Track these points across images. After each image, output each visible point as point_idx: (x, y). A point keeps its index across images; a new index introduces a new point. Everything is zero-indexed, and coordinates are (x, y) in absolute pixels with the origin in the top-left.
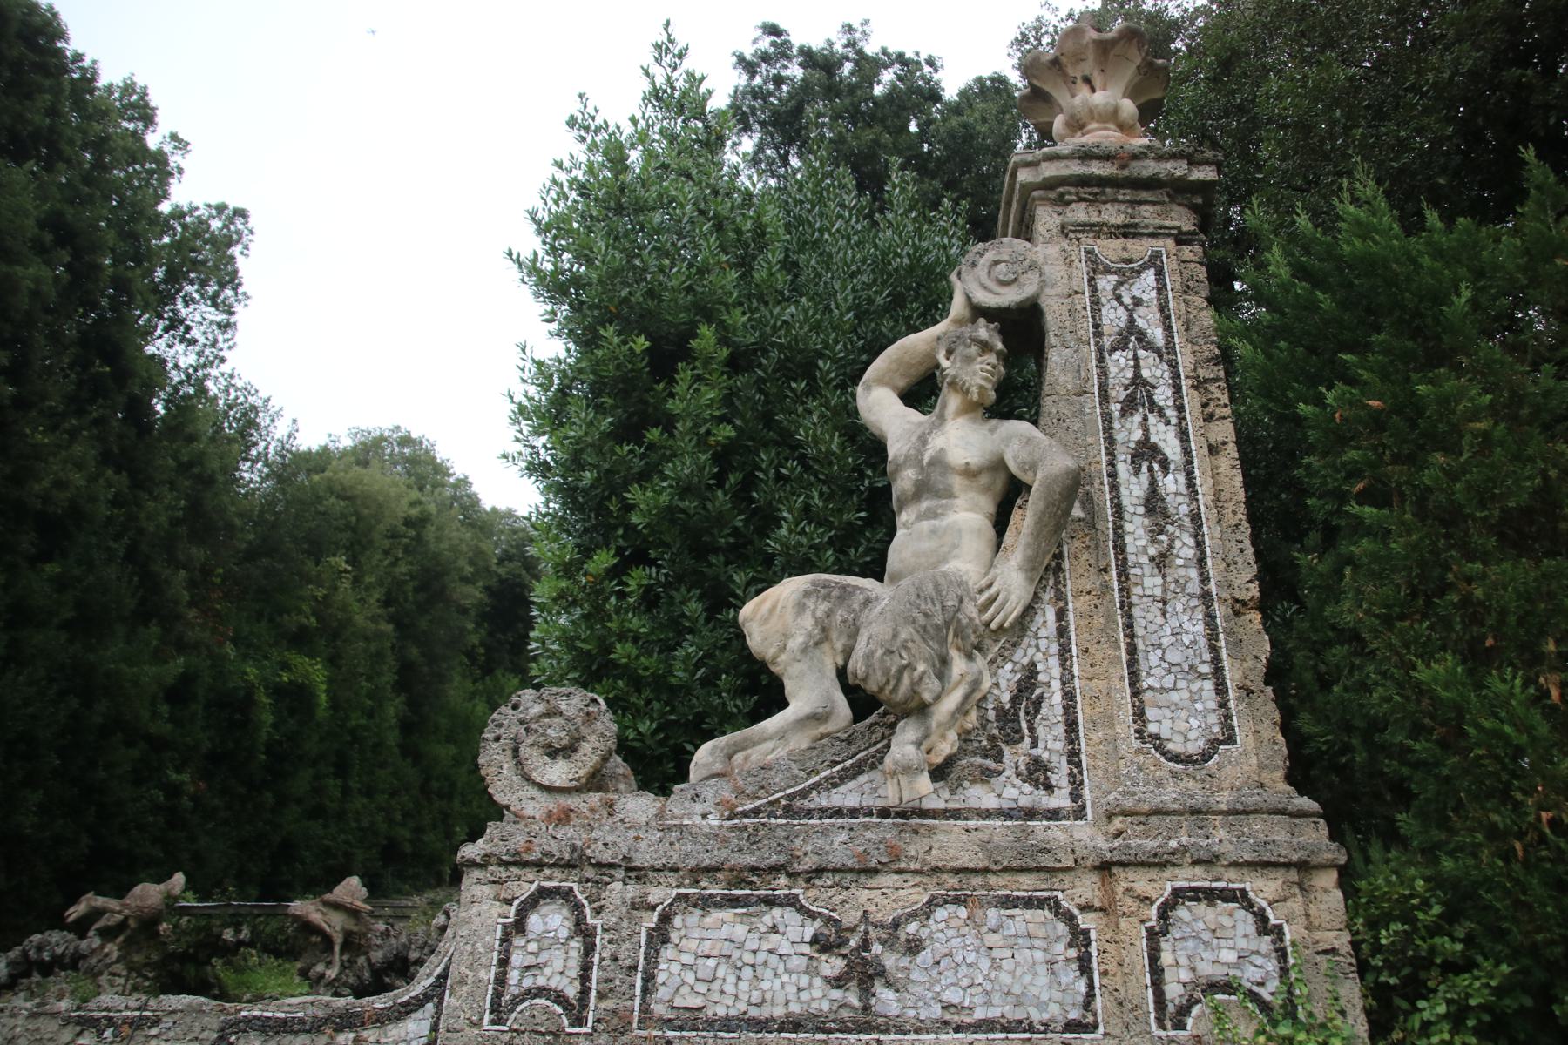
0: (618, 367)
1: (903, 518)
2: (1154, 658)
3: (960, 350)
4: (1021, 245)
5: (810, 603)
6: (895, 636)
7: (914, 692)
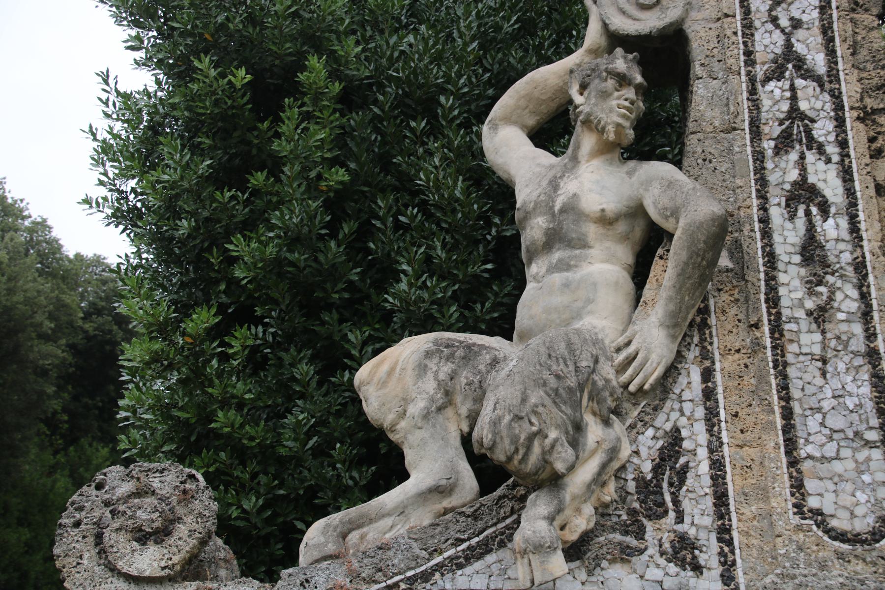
0: (216, 103)
1: (534, 270)
2: (813, 423)
3: (595, 84)
5: (432, 364)
6: (524, 400)
7: (546, 461)
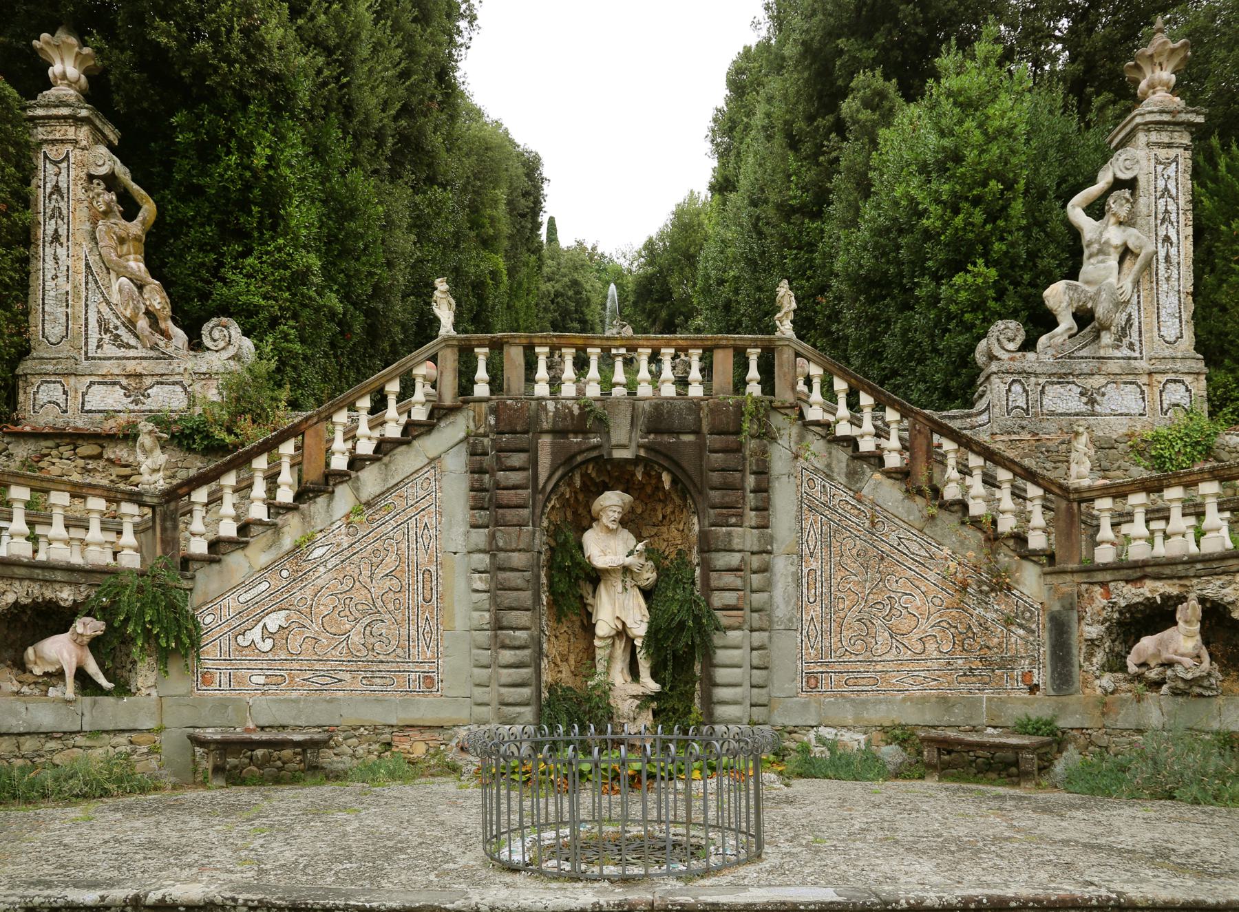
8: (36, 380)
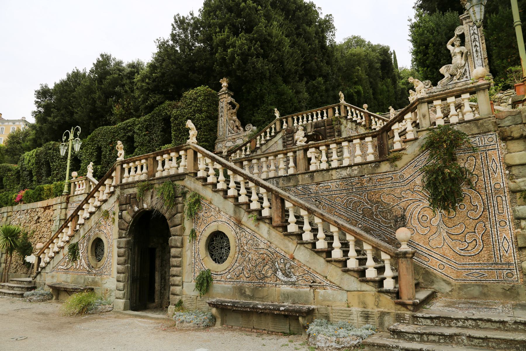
4: (461, 26)
8: (218, 143)
